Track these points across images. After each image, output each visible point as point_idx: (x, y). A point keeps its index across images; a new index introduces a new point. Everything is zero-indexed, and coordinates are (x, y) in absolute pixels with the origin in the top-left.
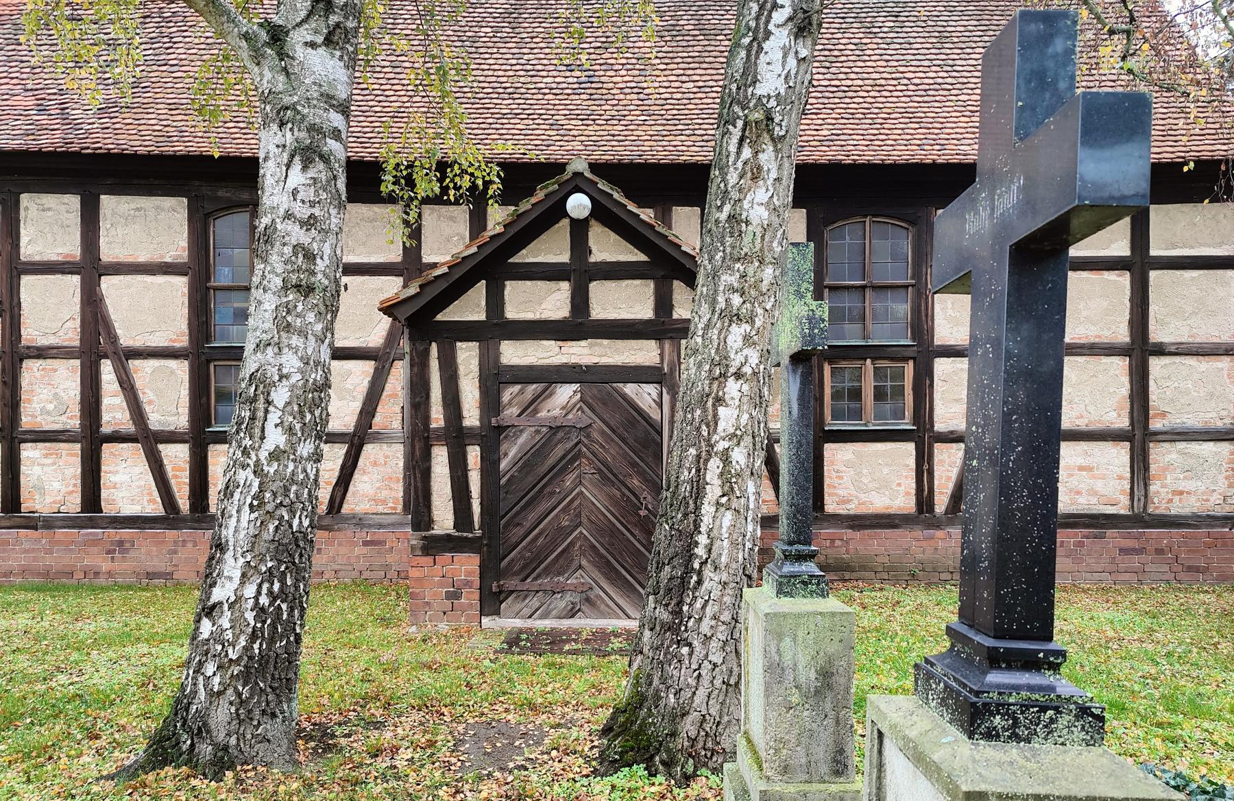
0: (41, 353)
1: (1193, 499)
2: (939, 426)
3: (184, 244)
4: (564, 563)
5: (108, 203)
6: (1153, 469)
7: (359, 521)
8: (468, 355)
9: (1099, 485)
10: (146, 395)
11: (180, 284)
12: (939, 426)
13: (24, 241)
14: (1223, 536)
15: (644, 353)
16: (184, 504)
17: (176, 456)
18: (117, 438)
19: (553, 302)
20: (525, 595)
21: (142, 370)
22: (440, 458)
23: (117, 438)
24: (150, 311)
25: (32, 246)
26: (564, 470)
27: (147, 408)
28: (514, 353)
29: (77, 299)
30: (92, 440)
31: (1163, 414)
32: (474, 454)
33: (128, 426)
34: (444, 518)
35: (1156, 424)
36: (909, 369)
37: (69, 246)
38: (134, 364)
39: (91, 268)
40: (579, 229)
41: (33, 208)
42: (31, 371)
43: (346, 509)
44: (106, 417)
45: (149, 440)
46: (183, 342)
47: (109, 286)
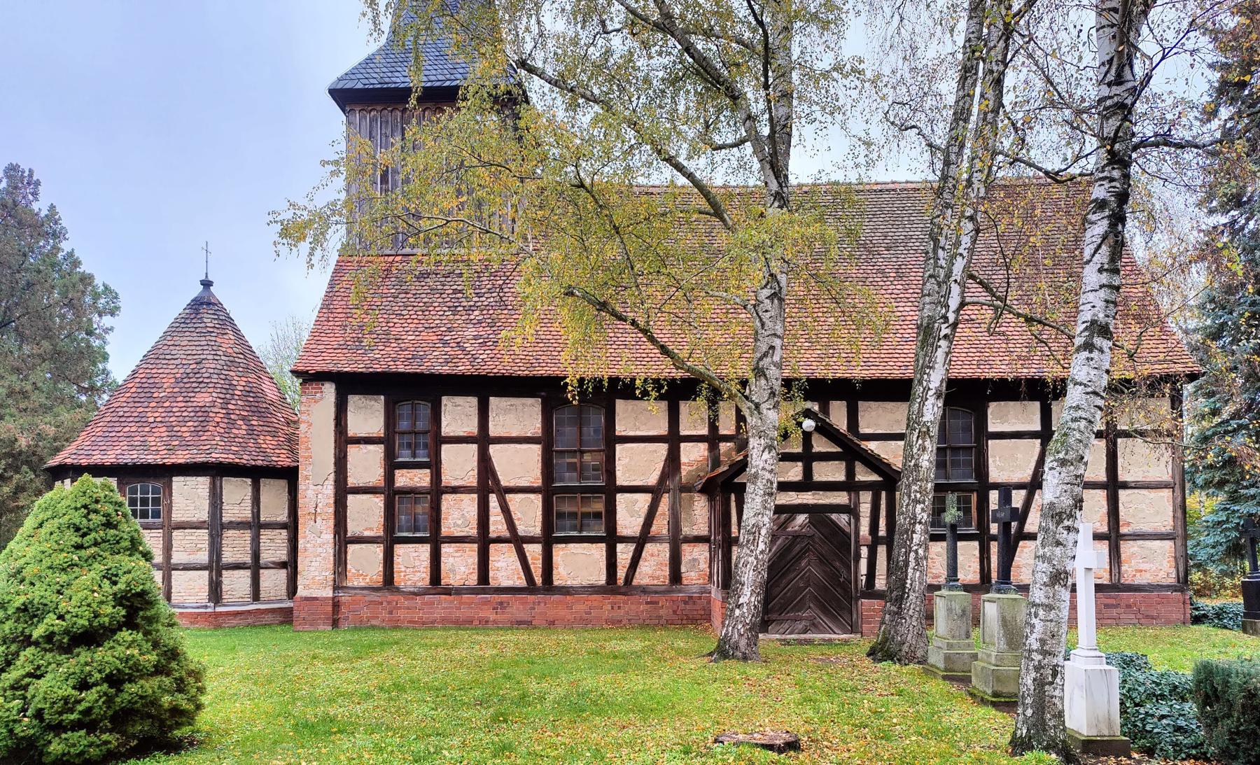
0: (455, 490)
1: (1148, 575)
3: (539, 425)
4: (800, 606)
5: (493, 401)
6: (1123, 557)
7: (644, 590)
10: (516, 514)
14: (1167, 597)
15: (841, 498)
16: (538, 580)
17: (534, 552)
18: (499, 540)
20: (782, 621)
21: (514, 500)
23: (499, 540)
24: (519, 465)
25: (449, 426)
26: (801, 558)
27: (517, 523)
29: (476, 458)
30: (484, 541)
31: (1129, 524)
35: (1123, 530)
36: (974, 497)
37: (472, 427)
38: (509, 497)
39: (483, 440)
40: (807, 436)
41: (449, 404)
42: (447, 501)
43: (635, 582)
44: (492, 528)
45: (518, 541)
46: (538, 483)
47: (493, 450)
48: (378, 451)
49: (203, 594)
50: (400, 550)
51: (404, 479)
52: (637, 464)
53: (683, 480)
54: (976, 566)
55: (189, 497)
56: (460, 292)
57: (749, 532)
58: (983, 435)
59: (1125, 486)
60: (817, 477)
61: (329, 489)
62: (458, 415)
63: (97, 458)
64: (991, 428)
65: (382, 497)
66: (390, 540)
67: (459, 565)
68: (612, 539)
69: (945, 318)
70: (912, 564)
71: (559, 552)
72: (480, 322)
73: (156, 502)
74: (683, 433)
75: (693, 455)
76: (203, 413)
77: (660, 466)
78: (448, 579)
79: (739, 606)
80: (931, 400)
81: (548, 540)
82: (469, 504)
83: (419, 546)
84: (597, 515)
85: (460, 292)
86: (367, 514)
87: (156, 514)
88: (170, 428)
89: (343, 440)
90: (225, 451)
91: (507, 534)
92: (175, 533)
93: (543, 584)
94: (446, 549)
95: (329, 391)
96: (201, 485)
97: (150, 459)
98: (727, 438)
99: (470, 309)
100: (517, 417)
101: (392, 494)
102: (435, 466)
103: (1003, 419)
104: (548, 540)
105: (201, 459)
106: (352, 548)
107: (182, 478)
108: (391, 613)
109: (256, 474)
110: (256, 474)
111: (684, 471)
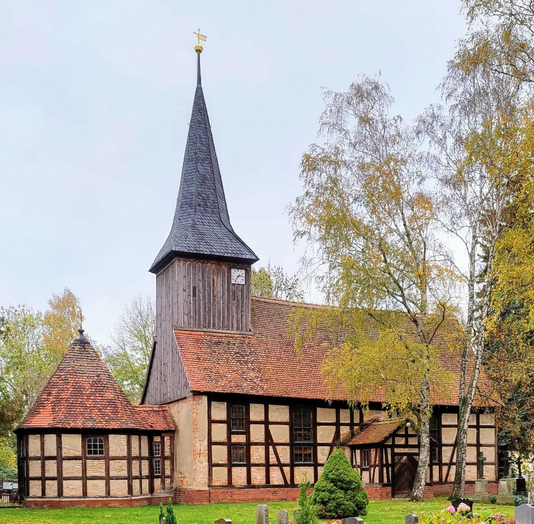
0: (256, 444)
2: (443, 462)
3: (288, 417)
5: (270, 406)
8: (389, 450)
9: (472, 475)
11: (287, 427)
12: (443, 462)
13: (251, 415)
16: (289, 482)
17: (287, 470)
18: (274, 465)
19: (402, 441)
21: (279, 448)
22: (385, 469)
23: (274, 465)
24: (281, 434)
25: (252, 418)
28: (397, 450)
30: (267, 465)
32: (390, 468)
36: (437, 449)
37: (262, 418)
38: (277, 447)
39: (266, 423)
41: (253, 407)
42: (253, 448)
44: (271, 460)
45: (281, 466)
46: (288, 441)
47: (271, 427)
48: (225, 426)
49: (125, 491)
50: (234, 469)
51: (235, 439)
52: (324, 434)
53: (341, 441)
54: (438, 475)
55: (117, 445)
56: (238, 353)
57: (424, 463)
58: (440, 426)
60: (409, 443)
61: (206, 443)
62: (256, 412)
63: (73, 425)
64: (443, 423)
65: (226, 447)
66: (230, 465)
67: (258, 476)
68: (316, 465)
69: (470, 398)
70: (463, 472)
71: (297, 470)
72: (253, 369)
73: (101, 446)
74: (341, 422)
75: (345, 431)
76: (111, 402)
77: (333, 435)
78: (254, 482)
79: (421, 486)
80: (466, 422)
81: (292, 466)
82: (261, 450)
83: (242, 467)
84: (310, 455)
85: (238, 353)
86: (221, 454)
87: (101, 452)
88: (100, 410)
89: (211, 421)
90: (132, 423)
91: (276, 463)
92: (111, 462)
93: (290, 484)
94: (253, 469)
95: (205, 399)
96: (122, 439)
97: (99, 426)
98: (356, 425)
99: (246, 362)
100: (280, 413)
101: (231, 446)
102: (247, 433)
104: (292, 466)
105: (125, 427)
106: (214, 469)
107: (113, 435)
108: (231, 496)
109: (139, 433)
110: (139, 433)
111: (342, 437)
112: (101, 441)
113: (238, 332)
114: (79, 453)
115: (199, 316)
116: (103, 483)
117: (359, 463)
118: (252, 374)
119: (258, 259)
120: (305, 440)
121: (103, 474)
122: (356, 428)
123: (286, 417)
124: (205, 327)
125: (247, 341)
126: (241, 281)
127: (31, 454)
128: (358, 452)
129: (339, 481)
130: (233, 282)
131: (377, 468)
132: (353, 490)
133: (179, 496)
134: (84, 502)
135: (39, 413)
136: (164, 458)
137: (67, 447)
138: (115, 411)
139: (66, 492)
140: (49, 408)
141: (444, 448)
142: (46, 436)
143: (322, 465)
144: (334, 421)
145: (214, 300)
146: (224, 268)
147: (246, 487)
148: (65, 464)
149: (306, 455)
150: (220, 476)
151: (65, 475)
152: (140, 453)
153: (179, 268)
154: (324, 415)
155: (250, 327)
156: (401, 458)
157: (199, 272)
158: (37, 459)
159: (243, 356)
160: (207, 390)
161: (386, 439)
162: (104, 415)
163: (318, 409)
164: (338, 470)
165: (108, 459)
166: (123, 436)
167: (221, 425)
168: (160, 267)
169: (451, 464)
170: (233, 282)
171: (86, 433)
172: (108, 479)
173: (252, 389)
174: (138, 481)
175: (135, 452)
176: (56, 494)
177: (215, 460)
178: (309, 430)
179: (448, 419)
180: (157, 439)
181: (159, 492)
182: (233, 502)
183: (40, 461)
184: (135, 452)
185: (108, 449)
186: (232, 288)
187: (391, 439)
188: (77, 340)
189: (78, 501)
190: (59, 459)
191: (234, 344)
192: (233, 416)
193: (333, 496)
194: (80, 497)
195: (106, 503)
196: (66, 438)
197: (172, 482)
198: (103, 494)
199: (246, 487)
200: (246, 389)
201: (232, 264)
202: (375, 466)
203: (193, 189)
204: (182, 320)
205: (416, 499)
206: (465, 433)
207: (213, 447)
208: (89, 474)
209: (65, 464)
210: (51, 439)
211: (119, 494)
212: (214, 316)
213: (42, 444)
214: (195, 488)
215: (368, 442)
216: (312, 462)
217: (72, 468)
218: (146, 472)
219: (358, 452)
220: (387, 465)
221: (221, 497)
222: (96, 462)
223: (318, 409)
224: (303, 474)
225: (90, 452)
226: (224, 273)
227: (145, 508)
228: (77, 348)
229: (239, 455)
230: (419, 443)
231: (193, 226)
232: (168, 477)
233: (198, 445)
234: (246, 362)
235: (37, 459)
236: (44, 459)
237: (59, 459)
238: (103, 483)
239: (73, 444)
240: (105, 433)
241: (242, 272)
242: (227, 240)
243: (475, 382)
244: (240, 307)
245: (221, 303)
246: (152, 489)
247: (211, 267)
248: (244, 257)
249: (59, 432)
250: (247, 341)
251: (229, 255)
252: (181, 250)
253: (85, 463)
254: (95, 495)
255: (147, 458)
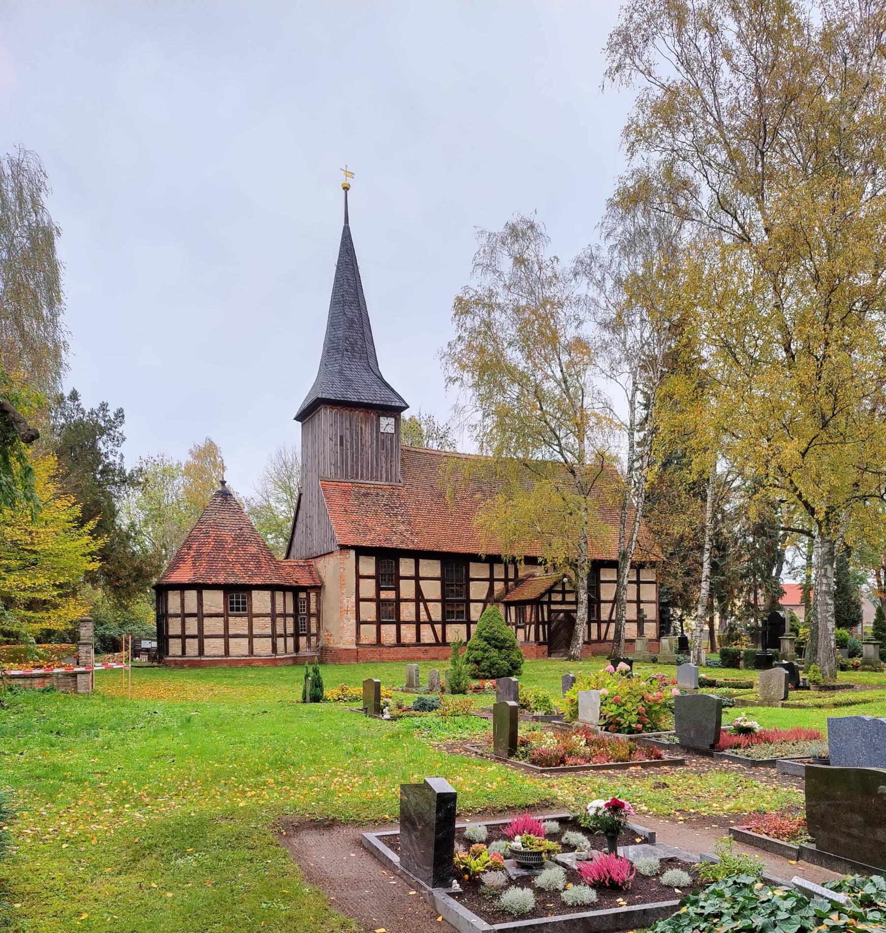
8: (545, 607)
10: (431, 612)
11: (439, 583)
16: (440, 640)
17: (438, 627)
18: (425, 623)
19: (559, 598)
22: (541, 626)
23: (425, 623)
24: (432, 590)
25: (402, 573)
28: (553, 607)
30: (418, 623)
33: (427, 620)
34: (541, 639)
37: (412, 573)
39: (417, 578)
42: (403, 605)
45: (432, 623)
46: (440, 598)
47: (421, 583)
48: (373, 581)
50: (383, 627)
51: (384, 595)
52: (478, 590)
54: (596, 633)
55: (260, 601)
58: (599, 582)
59: (642, 602)
61: (353, 599)
62: (406, 567)
63: (214, 580)
64: (602, 579)
66: (379, 623)
67: (408, 634)
68: (469, 623)
72: (403, 522)
73: (244, 603)
75: (499, 586)
76: (253, 556)
77: (486, 591)
78: (404, 640)
81: (444, 623)
82: (412, 606)
84: (462, 612)
86: (369, 611)
87: (244, 609)
88: (242, 565)
89: (359, 577)
92: (254, 619)
93: (442, 642)
94: (403, 627)
95: (352, 553)
96: (267, 594)
97: (242, 581)
98: (511, 580)
99: (396, 515)
100: (431, 568)
101: (380, 603)
102: (397, 589)
103: (605, 576)
104: (444, 623)
106: (362, 626)
109: (283, 588)
110: (283, 588)
111: (496, 593)
112: (243, 597)
113: (387, 483)
114: (221, 610)
115: (346, 466)
116: (245, 641)
117: (513, 621)
118: (402, 527)
119: (408, 407)
120: (457, 596)
121: (246, 632)
122: (510, 583)
123: (437, 573)
124: (353, 478)
125: (396, 493)
126: (391, 430)
127: (171, 611)
128: (513, 609)
129: (493, 639)
130: (382, 431)
131: (533, 626)
132: (508, 648)
133: (326, 655)
134: (226, 661)
135: (179, 568)
136: (310, 615)
137: (209, 603)
138: (259, 566)
139: (207, 651)
140: (189, 562)
141: (602, 605)
142: (186, 592)
143: (475, 622)
144: (487, 576)
145: (362, 449)
146: (373, 416)
147: (395, 646)
148: (207, 621)
149: (458, 612)
150: (369, 634)
151: (206, 633)
152: (285, 610)
153: (325, 416)
154: (477, 570)
155: (400, 478)
156: (558, 615)
157: (346, 420)
158: (177, 616)
159: (392, 508)
160: (355, 543)
161: (543, 595)
162: (247, 570)
163: (471, 564)
164: (491, 627)
165: (251, 616)
166: (266, 592)
167: (370, 580)
168: (306, 415)
169: (610, 621)
170: (382, 431)
171: (228, 589)
172: (251, 637)
173: (402, 543)
174: (282, 639)
175: (279, 609)
176: (197, 653)
177: (363, 617)
178: (461, 586)
179: (607, 575)
180: (303, 595)
181: (304, 651)
182: (382, 661)
183: (180, 619)
184: (279, 609)
185: (251, 606)
186: (381, 437)
187: (547, 596)
188: (218, 492)
189: (220, 660)
190: (200, 616)
191: (383, 496)
192: (382, 571)
193: (486, 655)
194: (222, 656)
195: (250, 662)
196: (206, 594)
197: (318, 640)
198: (246, 652)
199: (395, 646)
200: (396, 543)
201: (380, 412)
202: (530, 624)
203: (340, 333)
204: (329, 471)
205: (573, 658)
206: (625, 589)
207: (361, 603)
208: (231, 632)
209: (207, 621)
210: (191, 596)
211: (263, 653)
212: (362, 466)
213: (183, 600)
214: (342, 646)
215: (523, 598)
216: (464, 620)
217: (214, 626)
218: (290, 630)
219: (513, 609)
220: (543, 623)
221: (369, 656)
222: (239, 619)
223: (471, 564)
224: (456, 632)
225: (232, 609)
226: (372, 421)
227: (290, 668)
228: (219, 499)
229: (388, 612)
230: (577, 599)
231: (341, 372)
232: (314, 635)
233: (345, 601)
234: (396, 515)
235: (177, 616)
236: (184, 616)
237: (200, 616)
238: (245, 641)
239: (214, 601)
240: (248, 588)
241: (392, 420)
242: (376, 387)
243: (635, 535)
244: (389, 457)
245: (369, 453)
246: (297, 648)
247: (359, 415)
248: (393, 404)
249: (200, 587)
250: (396, 493)
251: (378, 402)
252: (328, 397)
253: (228, 620)
254: (237, 654)
255: (292, 616)
